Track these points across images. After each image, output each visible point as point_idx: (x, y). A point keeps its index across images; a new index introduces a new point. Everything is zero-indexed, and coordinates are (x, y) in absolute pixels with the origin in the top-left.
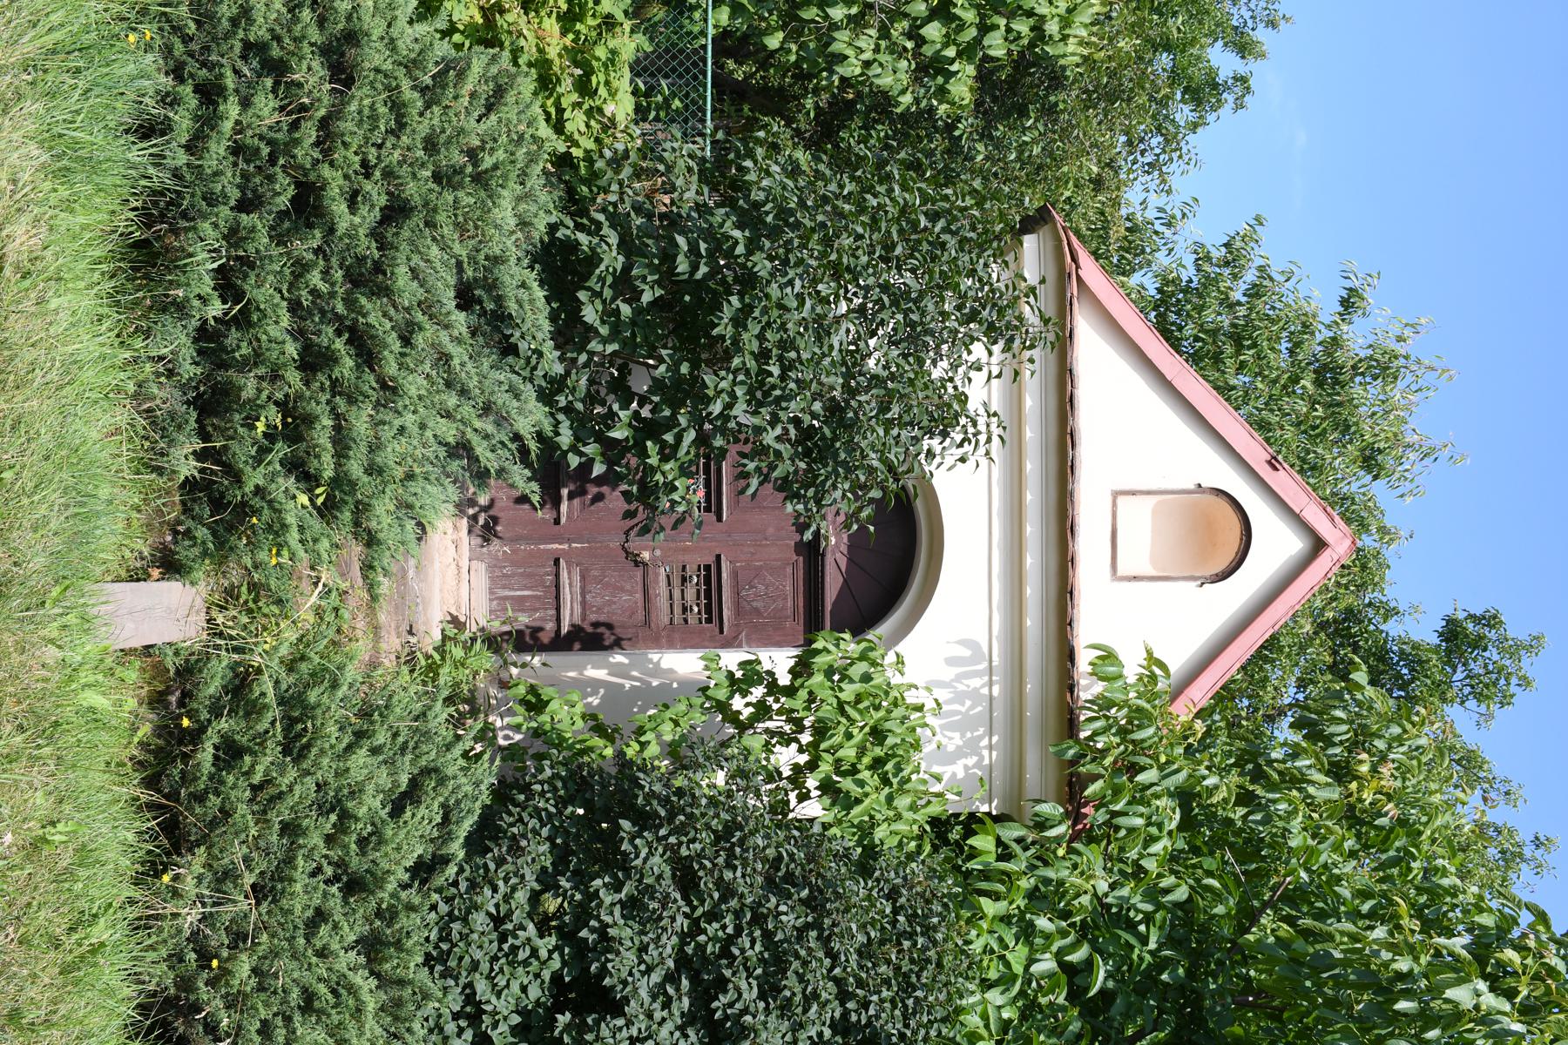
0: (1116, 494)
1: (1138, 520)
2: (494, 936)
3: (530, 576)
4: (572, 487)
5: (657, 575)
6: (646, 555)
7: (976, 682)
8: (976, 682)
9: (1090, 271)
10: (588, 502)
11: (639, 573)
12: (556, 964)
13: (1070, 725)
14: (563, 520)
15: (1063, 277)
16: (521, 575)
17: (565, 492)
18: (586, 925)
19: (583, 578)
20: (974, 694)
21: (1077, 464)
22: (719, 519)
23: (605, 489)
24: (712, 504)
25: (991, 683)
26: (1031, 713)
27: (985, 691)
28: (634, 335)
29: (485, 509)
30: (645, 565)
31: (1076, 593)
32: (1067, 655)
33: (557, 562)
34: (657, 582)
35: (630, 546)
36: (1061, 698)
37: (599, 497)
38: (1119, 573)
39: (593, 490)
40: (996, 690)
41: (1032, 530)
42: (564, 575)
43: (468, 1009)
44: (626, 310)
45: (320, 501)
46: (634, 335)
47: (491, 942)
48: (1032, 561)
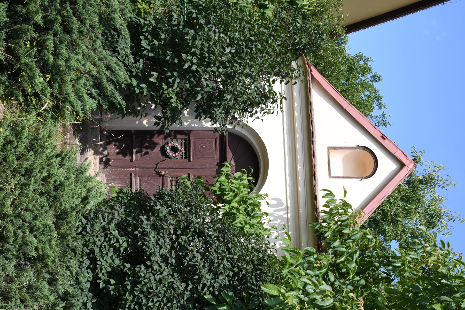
0: (330, 148)
1: (338, 160)
2: (103, 234)
3: (121, 179)
4: (137, 149)
5: (167, 180)
6: (163, 173)
7: (281, 213)
8: (281, 213)
9: (315, 73)
10: (143, 154)
11: (160, 179)
12: (125, 245)
13: (316, 219)
14: (134, 160)
15: (305, 72)
16: (118, 179)
17: (135, 151)
18: (137, 230)
19: (140, 181)
20: (280, 217)
21: (314, 132)
22: (189, 161)
23: (149, 150)
24: (187, 155)
25: (287, 213)
26: (302, 211)
27: (285, 216)
28: (159, 51)
29: (106, 156)
30: (163, 176)
31: (316, 175)
32: (314, 198)
33: (131, 174)
34: (167, 182)
35: (158, 170)
36: (313, 213)
37: (147, 153)
38: (332, 175)
39: (144, 151)
40: (289, 215)
41: (299, 156)
42: (133, 179)
43: (91, 266)
44: (156, 42)
45: (48, 79)
46: (159, 51)
47: (101, 237)
48: (300, 167)
